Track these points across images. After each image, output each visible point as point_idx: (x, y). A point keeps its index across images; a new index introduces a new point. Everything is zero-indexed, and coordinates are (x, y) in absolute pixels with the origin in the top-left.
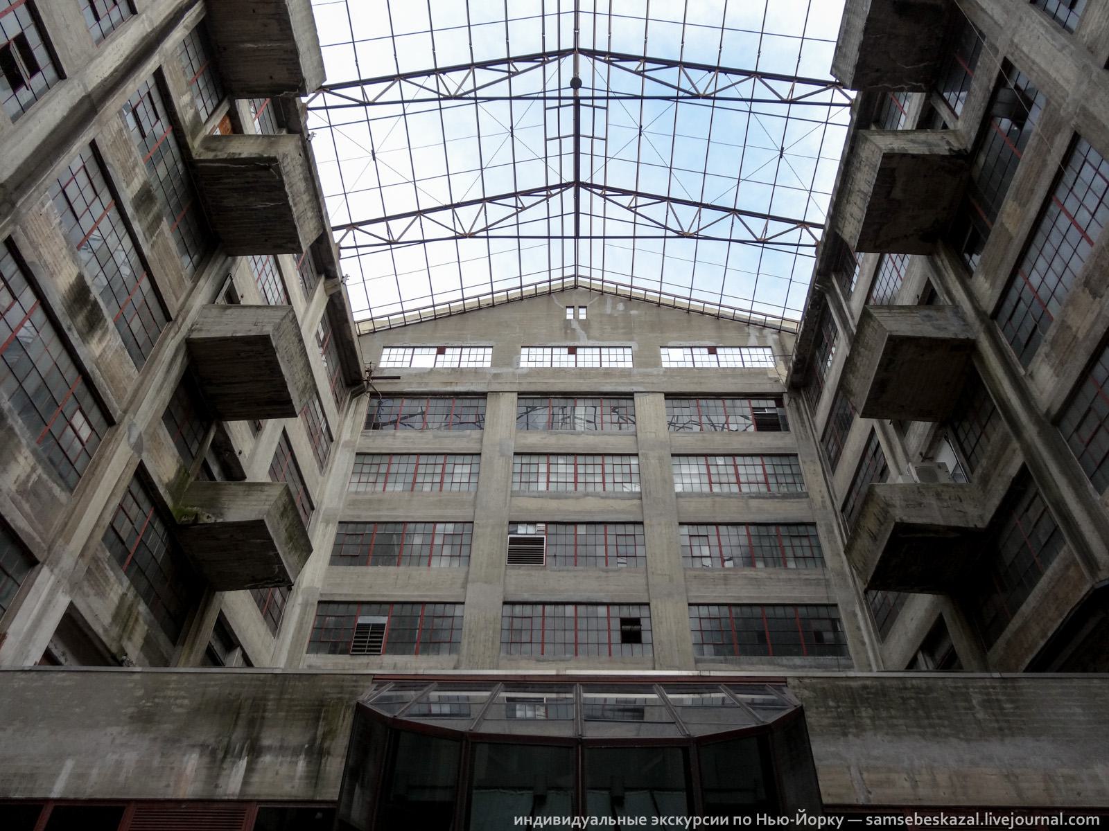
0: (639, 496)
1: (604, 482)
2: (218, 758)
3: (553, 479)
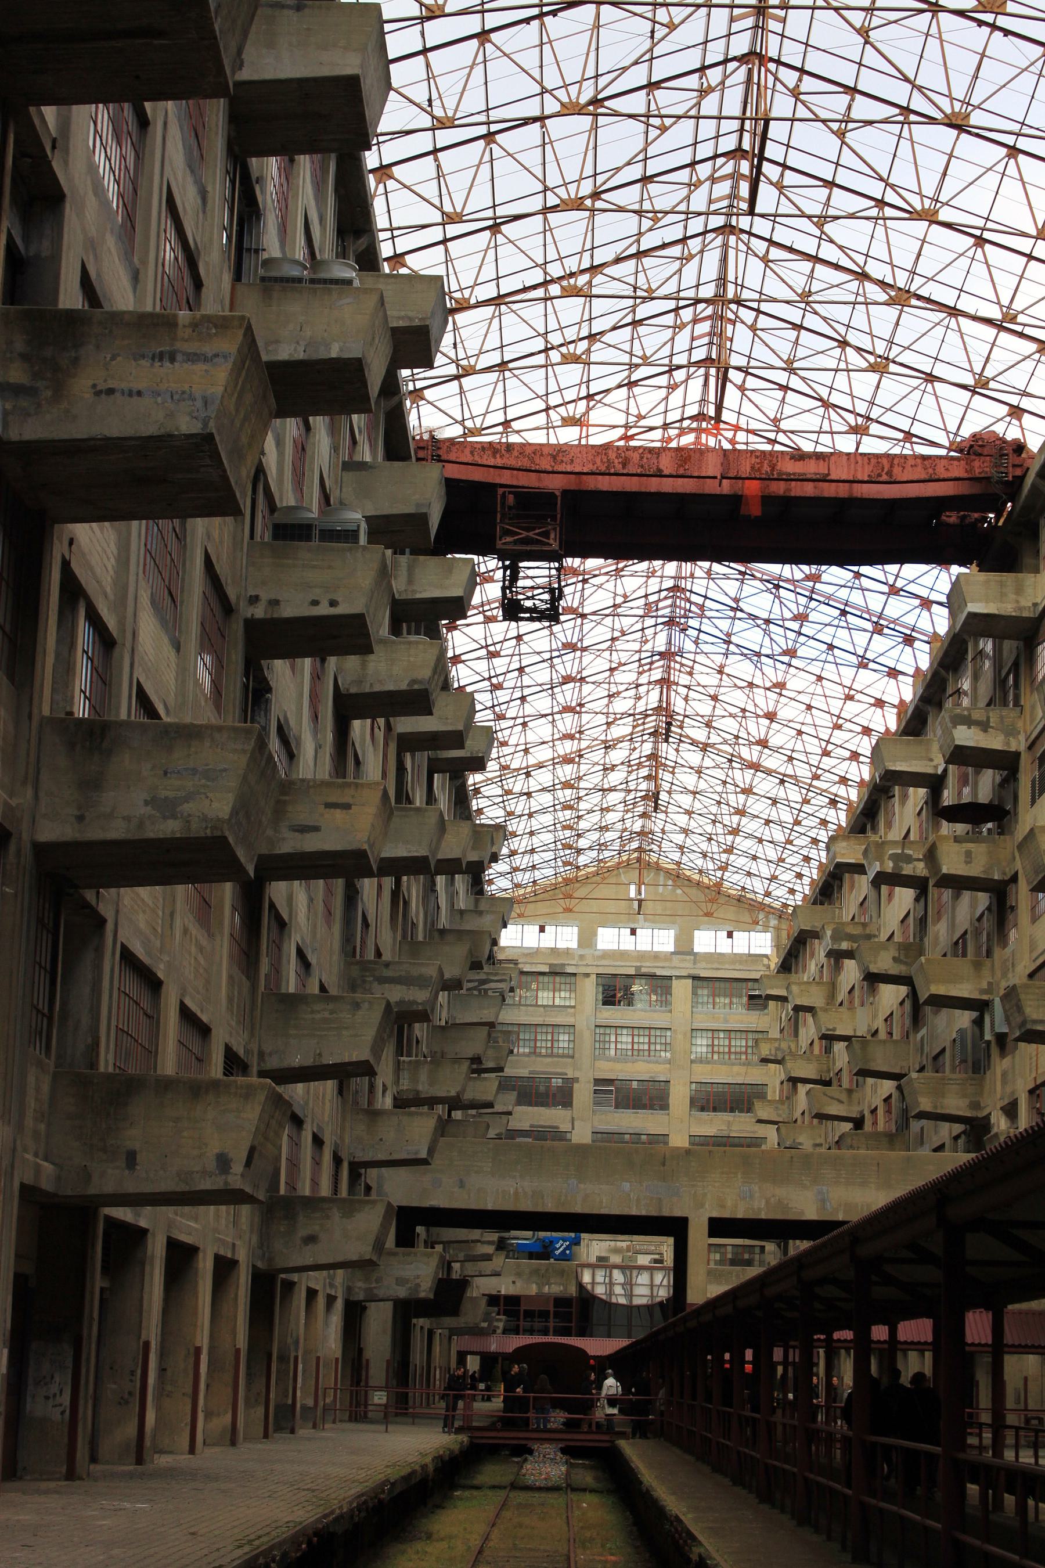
0: (669, 1062)
1: (649, 1050)
2: (540, 1286)
3: (619, 1046)
